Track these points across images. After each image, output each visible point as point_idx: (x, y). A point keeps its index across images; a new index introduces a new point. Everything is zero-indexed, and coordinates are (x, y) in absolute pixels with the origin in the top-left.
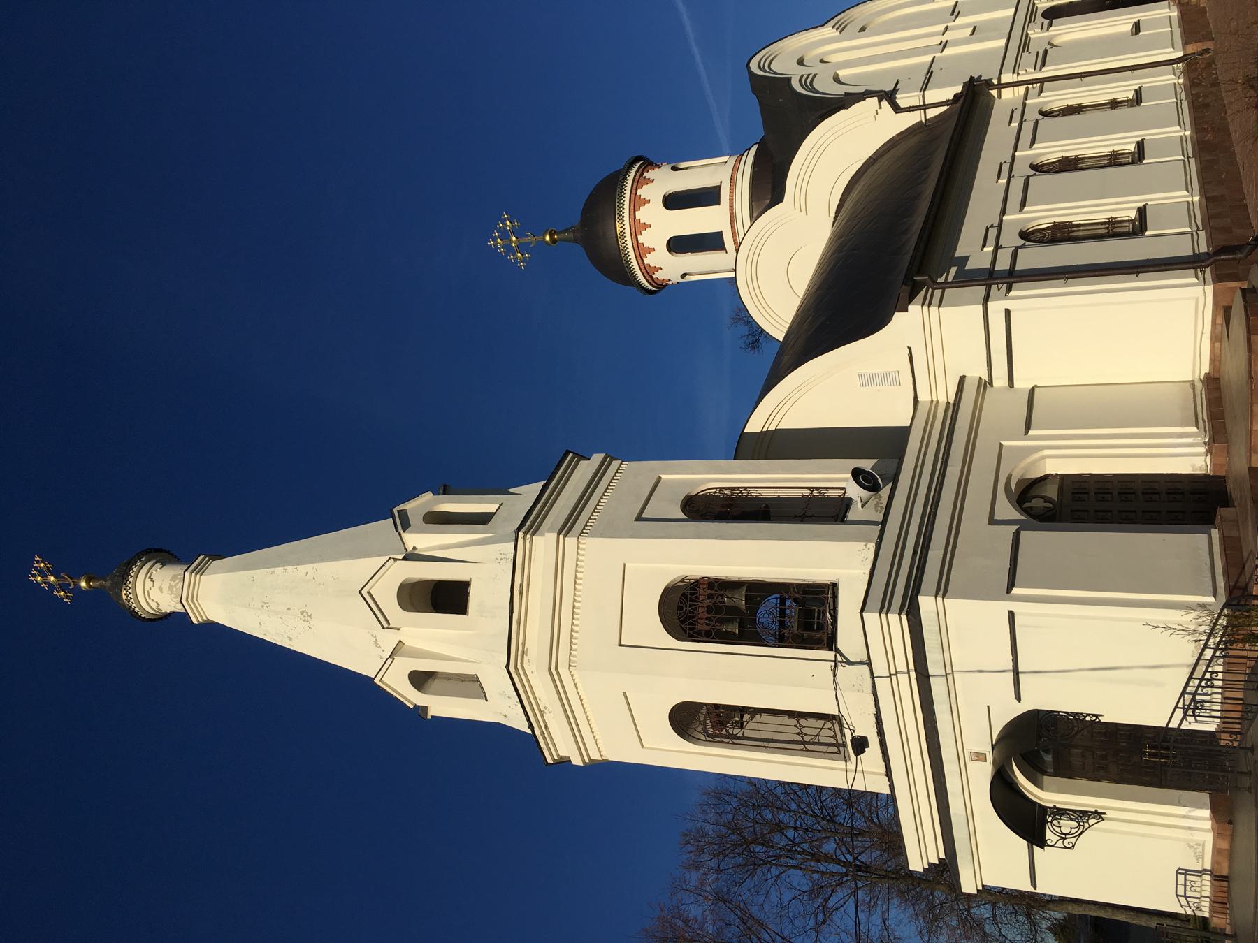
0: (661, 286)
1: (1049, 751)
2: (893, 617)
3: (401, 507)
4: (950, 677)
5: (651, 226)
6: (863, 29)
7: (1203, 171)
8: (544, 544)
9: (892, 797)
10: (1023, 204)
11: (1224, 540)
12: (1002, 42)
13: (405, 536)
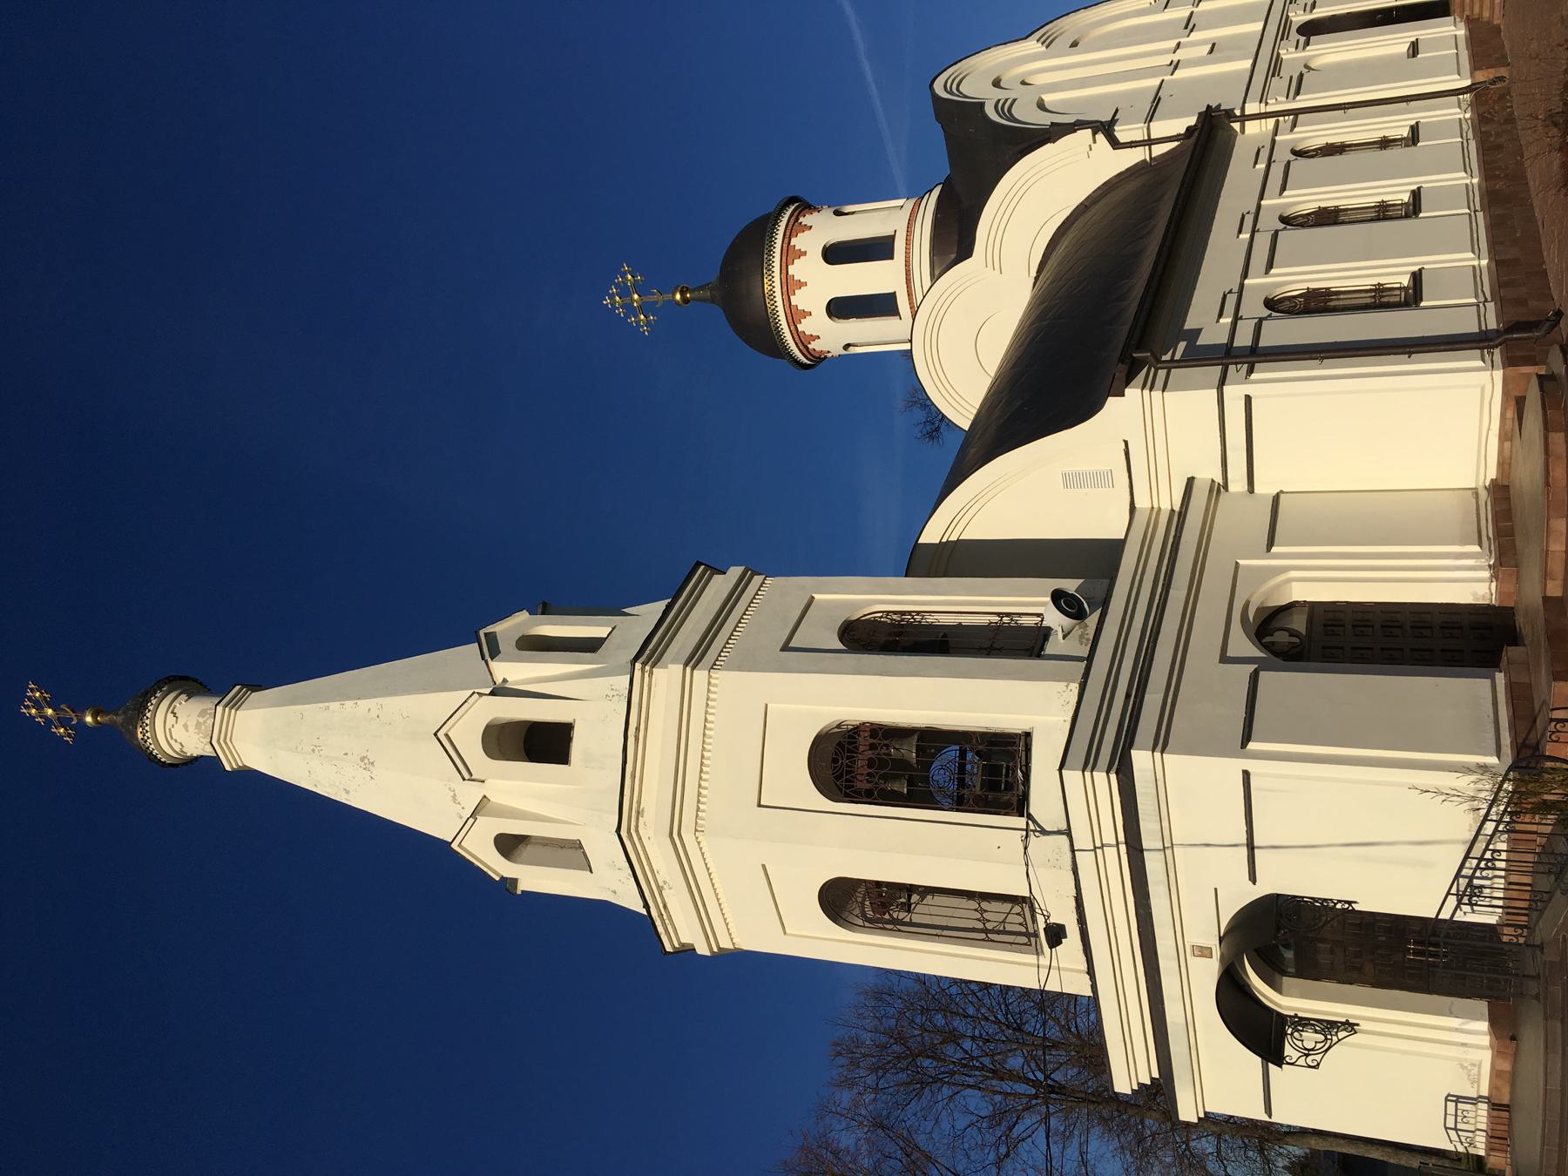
0: (819, 359)
1: (1291, 946)
2: (1100, 776)
3: (489, 629)
4: (1168, 852)
5: (807, 285)
6: (1075, 44)
7: (1494, 228)
8: (667, 677)
9: (1094, 1000)
11: (1511, 687)
12: (1248, 64)
13: (494, 665)
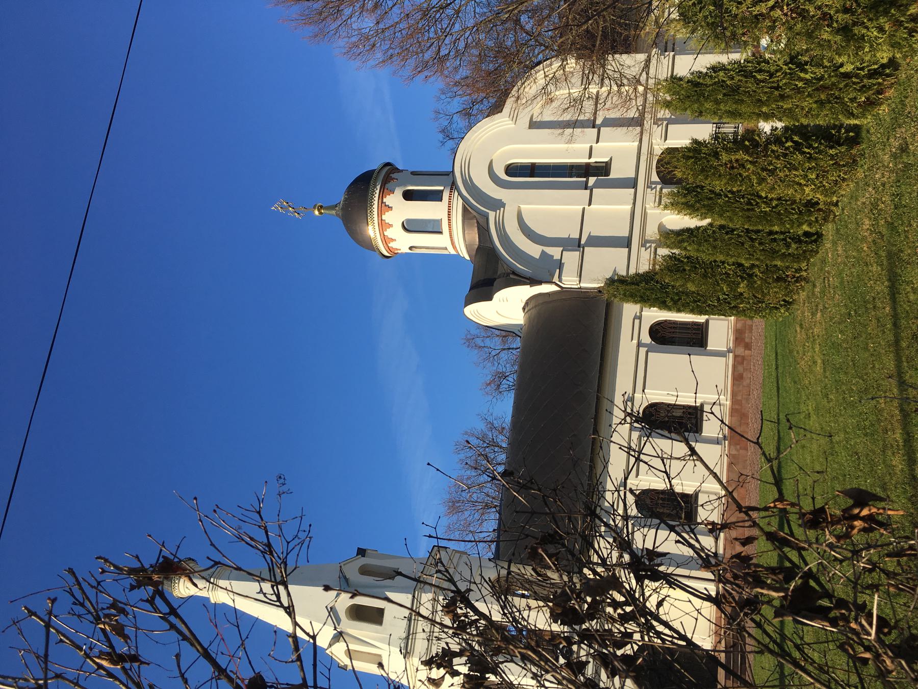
10: (637, 476)
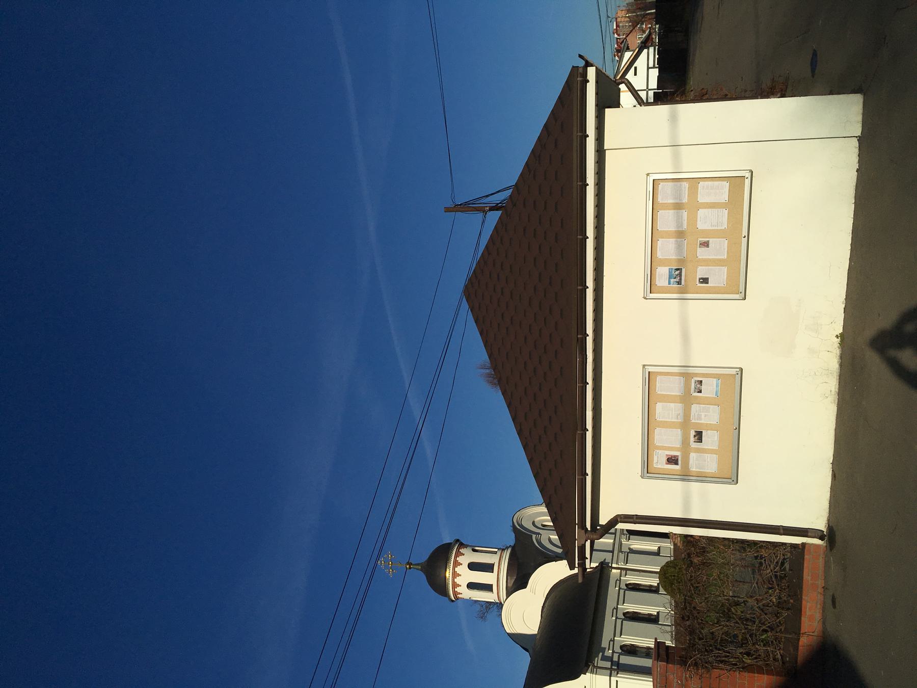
0: (457, 599)
5: (461, 576)
